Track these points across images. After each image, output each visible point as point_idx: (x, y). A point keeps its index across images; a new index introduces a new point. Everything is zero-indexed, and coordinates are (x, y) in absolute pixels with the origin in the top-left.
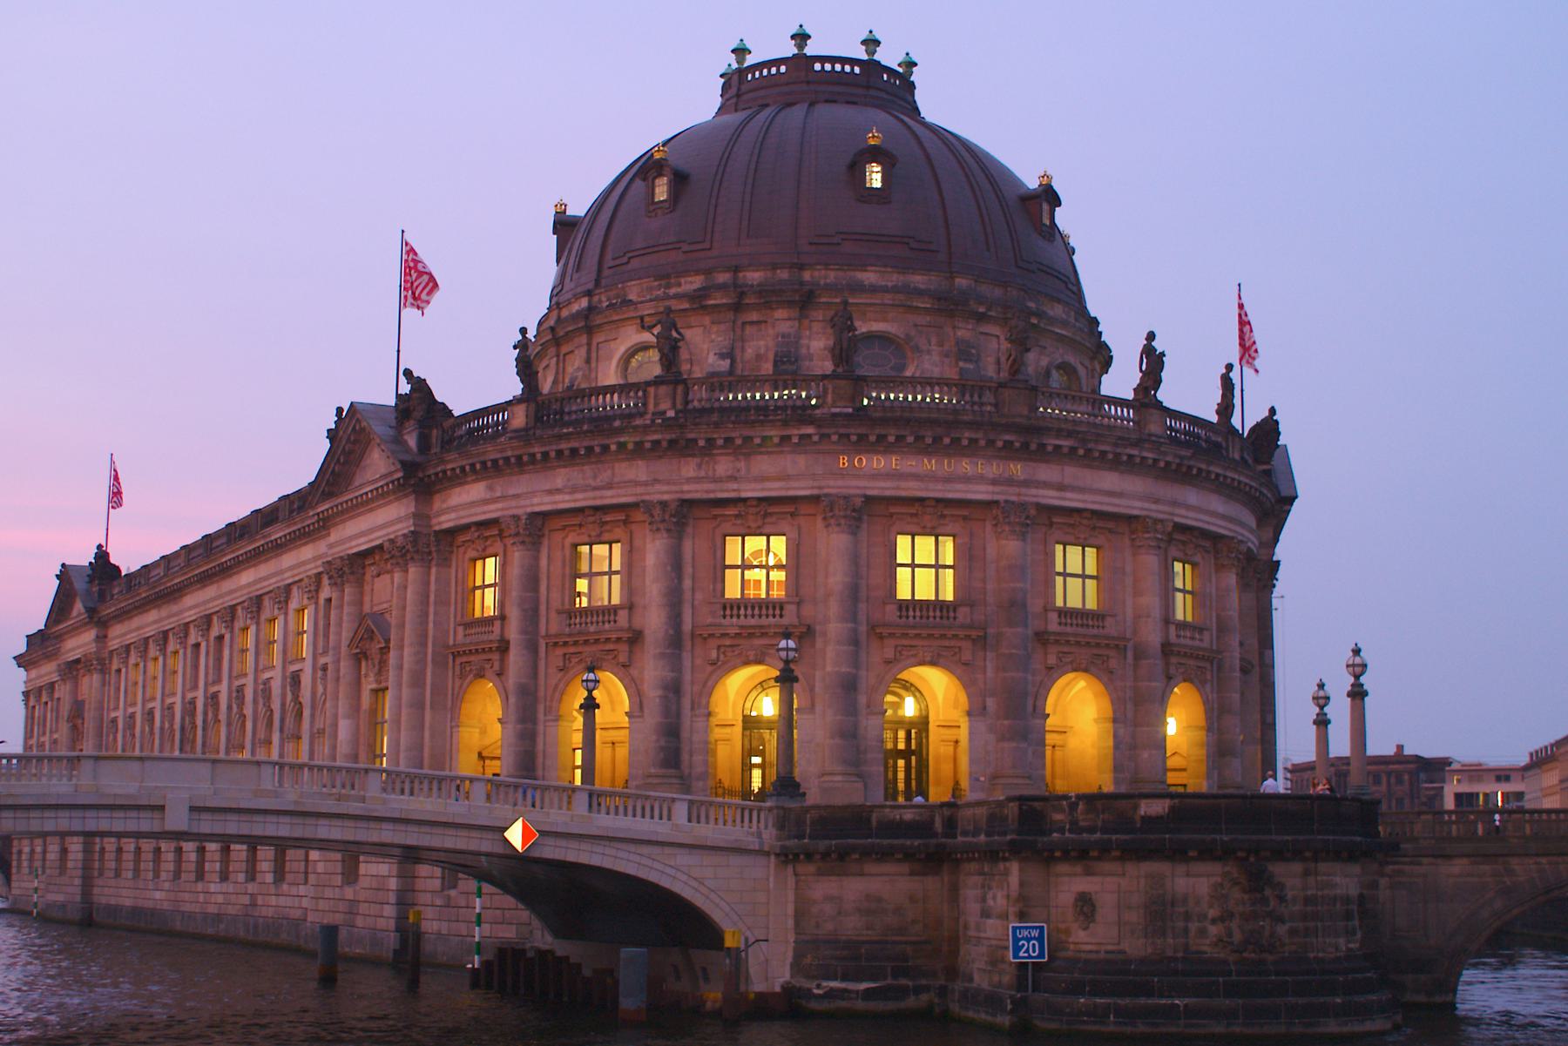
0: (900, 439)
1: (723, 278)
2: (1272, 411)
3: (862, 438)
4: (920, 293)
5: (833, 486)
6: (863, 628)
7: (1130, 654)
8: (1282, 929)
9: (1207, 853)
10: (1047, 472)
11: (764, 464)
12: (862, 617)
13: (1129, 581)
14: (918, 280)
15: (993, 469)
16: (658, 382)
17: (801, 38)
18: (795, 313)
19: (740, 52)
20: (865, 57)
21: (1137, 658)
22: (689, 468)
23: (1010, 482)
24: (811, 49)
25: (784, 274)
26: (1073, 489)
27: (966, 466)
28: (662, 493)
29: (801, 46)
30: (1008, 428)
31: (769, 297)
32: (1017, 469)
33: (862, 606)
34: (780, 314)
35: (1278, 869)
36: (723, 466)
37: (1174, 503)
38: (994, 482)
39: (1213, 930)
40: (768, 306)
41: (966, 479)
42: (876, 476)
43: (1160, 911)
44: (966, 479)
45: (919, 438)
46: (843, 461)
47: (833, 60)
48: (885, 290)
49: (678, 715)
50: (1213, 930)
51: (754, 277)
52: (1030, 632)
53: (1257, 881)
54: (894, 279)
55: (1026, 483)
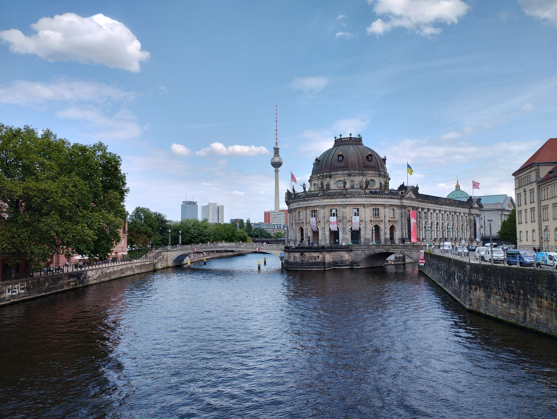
0: (328, 198)
1: (321, 174)
2: (404, 183)
3: (323, 198)
4: (345, 174)
5: (321, 204)
6: (326, 221)
7: (364, 222)
8: (305, 259)
9: (298, 252)
10: (348, 200)
11: (313, 202)
12: (326, 220)
13: (364, 212)
14: (346, 172)
15: (341, 200)
16: (303, 192)
17: (341, 136)
18: (329, 178)
19: (335, 138)
20: (349, 137)
21: (365, 222)
22: (306, 202)
23: (343, 202)
24: (342, 138)
25: (328, 173)
26: (352, 201)
27: (337, 200)
28: (304, 206)
29: (341, 137)
30: (341, 195)
31: (326, 177)
32: (344, 200)
33: (326, 218)
34: (328, 179)
35: (305, 253)
36: (310, 202)
37: (370, 201)
38: (341, 202)
39: (299, 259)
40: (326, 178)
41: (337, 202)
42: (325, 202)
43: (294, 257)
44: (337, 202)
45: (330, 197)
46: (322, 201)
47: (345, 138)
48: (341, 174)
49: (307, 232)
50: (299, 259)
51: (325, 174)
52: (347, 220)
53: (302, 255)
54: (342, 172)
55: (345, 202)
